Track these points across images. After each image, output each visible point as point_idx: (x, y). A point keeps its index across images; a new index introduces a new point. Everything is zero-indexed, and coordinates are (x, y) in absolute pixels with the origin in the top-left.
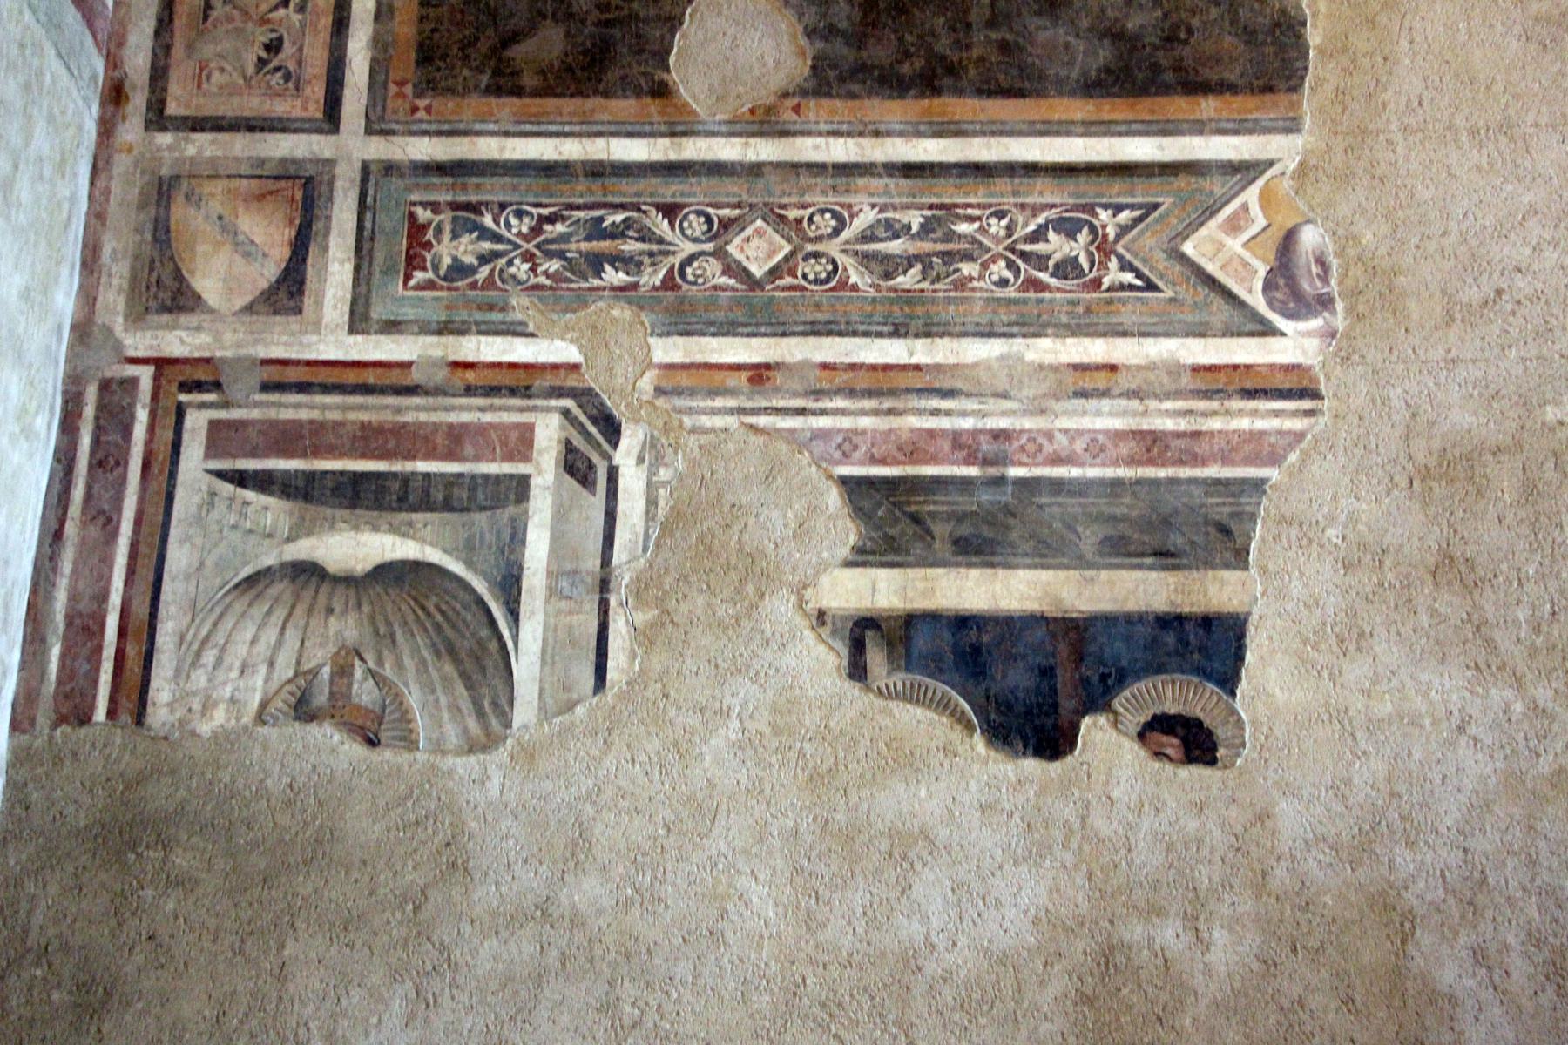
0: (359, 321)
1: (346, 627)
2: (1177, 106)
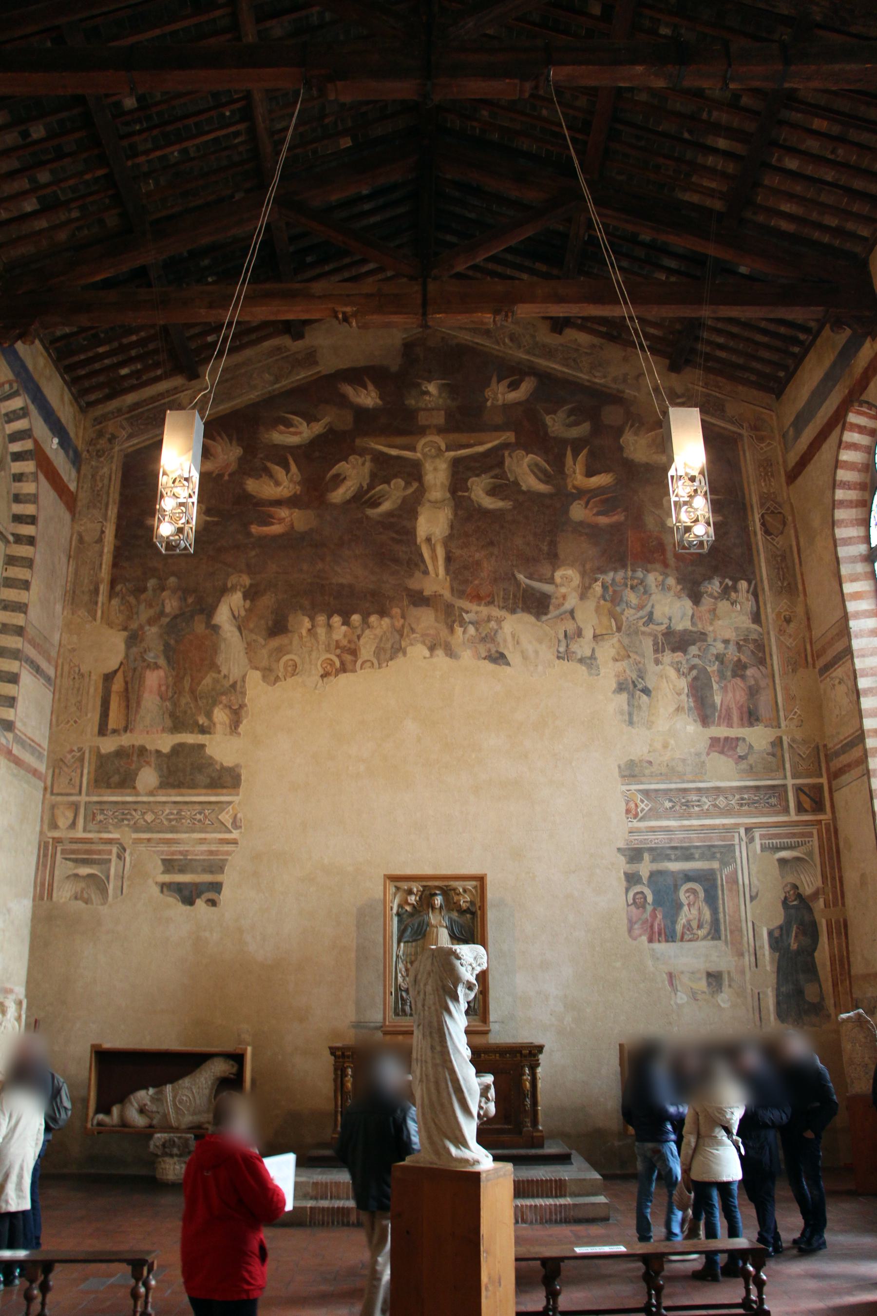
1: (82, 884)
2: (220, 791)
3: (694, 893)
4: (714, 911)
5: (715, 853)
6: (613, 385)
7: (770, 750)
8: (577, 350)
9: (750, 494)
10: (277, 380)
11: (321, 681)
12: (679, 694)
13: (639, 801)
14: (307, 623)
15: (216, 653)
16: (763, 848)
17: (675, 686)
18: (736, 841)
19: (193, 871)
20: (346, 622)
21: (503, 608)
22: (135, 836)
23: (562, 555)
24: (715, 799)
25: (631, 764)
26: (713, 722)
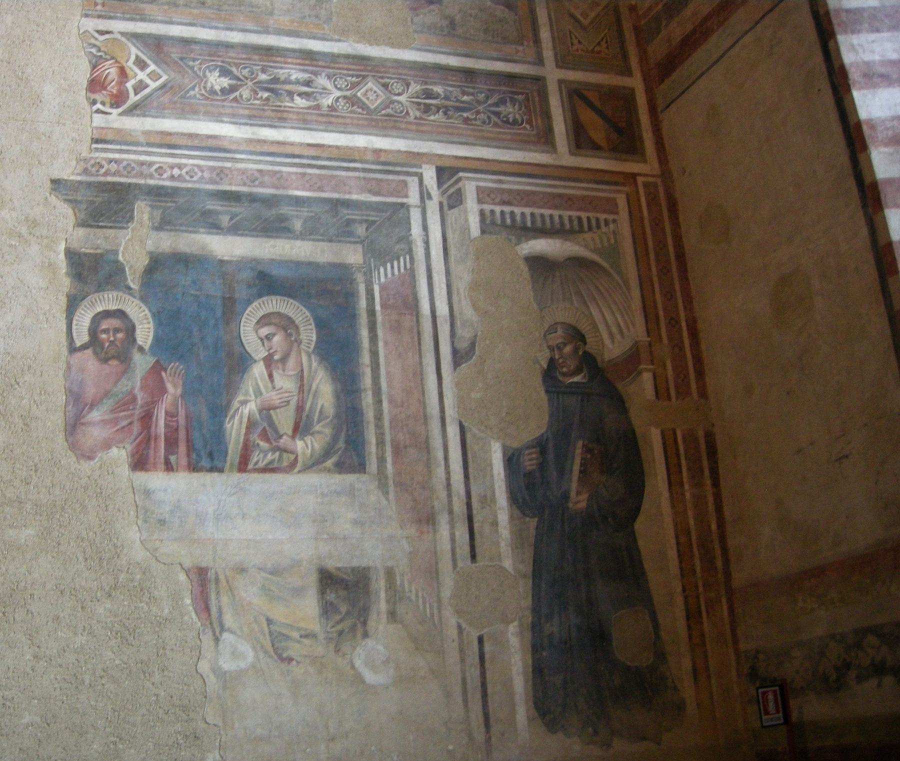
3: (285, 329)
13: (130, 63)
16: (487, 224)
24: (354, 86)
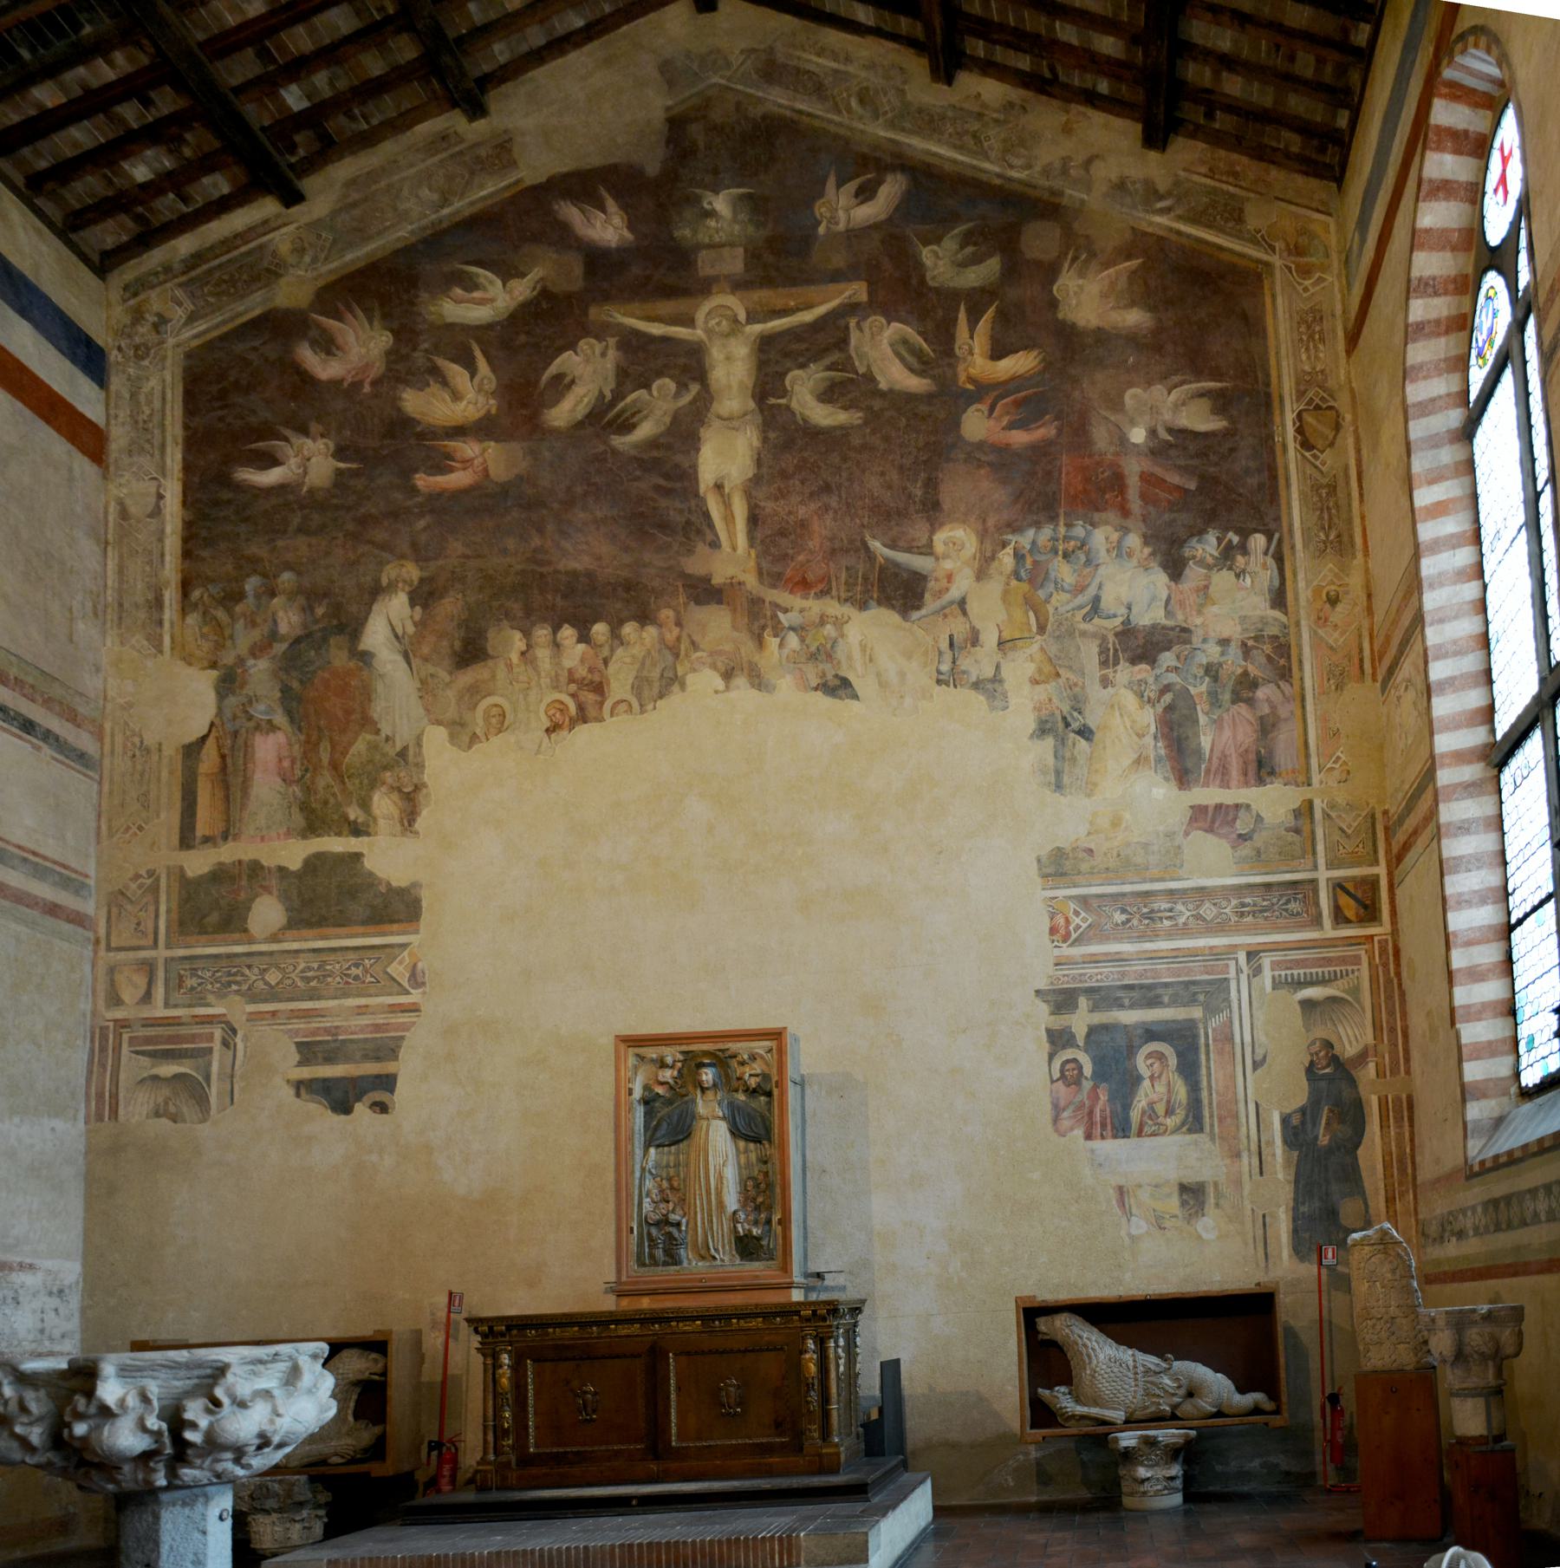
0: (167, 1005)
2: (387, 927)
4: (1194, 1088)
5: (1195, 994)
6: (1044, 182)
7: (1291, 821)
8: (980, 116)
9: (1279, 377)
10: (445, 202)
11: (546, 739)
12: (1140, 736)
14: (518, 641)
15: (370, 700)
16: (1276, 984)
17: (1134, 722)
18: (1232, 974)
19: (348, 1059)
20: (584, 638)
21: (846, 600)
22: (251, 1008)
23: (946, 505)
24: (1198, 907)
25: (1059, 854)
26: (1197, 781)
